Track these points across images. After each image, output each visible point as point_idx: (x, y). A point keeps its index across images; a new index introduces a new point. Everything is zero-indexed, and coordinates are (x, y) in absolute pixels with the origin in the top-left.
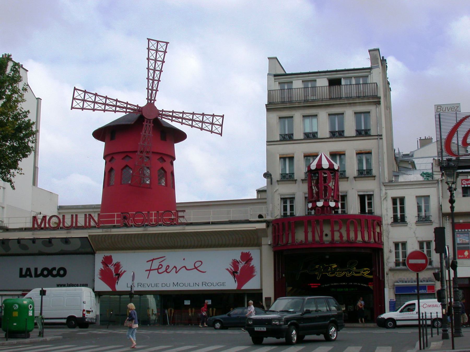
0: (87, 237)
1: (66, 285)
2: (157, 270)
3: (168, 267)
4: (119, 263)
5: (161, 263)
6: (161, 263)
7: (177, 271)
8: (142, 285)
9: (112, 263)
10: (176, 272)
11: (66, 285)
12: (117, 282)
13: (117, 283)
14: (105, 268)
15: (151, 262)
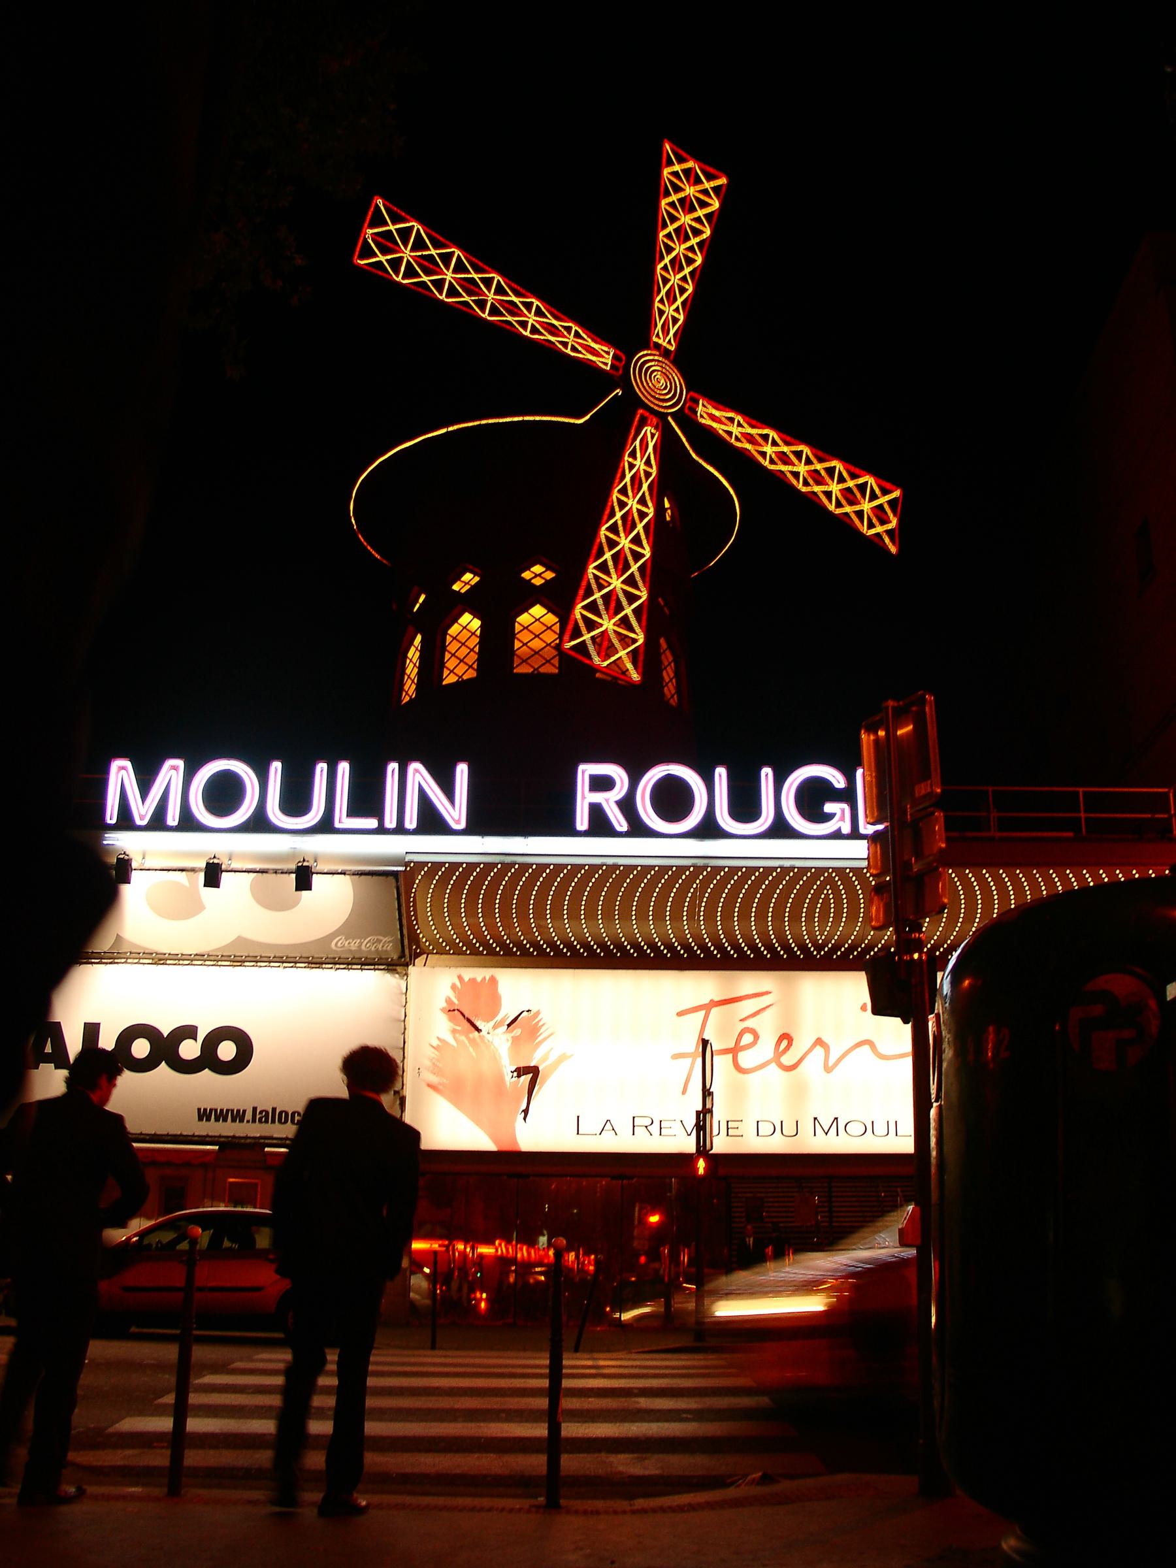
0: (395, 874)
1: (249, 1116)
2: (731, 1056)
3: (785, 1043)
4: (538, 1013)
5: (748, 1024)
6: (749, 1023)
7: (831, 1063)
8: (657, 1124)
9: (499, 1018)
10: (828, 1069)
11: (249, 1116)
12: (524, 1106)
13: (526, 1112)
14: (463, 1038)
15: (702, 1014)
